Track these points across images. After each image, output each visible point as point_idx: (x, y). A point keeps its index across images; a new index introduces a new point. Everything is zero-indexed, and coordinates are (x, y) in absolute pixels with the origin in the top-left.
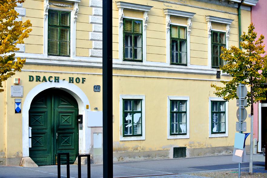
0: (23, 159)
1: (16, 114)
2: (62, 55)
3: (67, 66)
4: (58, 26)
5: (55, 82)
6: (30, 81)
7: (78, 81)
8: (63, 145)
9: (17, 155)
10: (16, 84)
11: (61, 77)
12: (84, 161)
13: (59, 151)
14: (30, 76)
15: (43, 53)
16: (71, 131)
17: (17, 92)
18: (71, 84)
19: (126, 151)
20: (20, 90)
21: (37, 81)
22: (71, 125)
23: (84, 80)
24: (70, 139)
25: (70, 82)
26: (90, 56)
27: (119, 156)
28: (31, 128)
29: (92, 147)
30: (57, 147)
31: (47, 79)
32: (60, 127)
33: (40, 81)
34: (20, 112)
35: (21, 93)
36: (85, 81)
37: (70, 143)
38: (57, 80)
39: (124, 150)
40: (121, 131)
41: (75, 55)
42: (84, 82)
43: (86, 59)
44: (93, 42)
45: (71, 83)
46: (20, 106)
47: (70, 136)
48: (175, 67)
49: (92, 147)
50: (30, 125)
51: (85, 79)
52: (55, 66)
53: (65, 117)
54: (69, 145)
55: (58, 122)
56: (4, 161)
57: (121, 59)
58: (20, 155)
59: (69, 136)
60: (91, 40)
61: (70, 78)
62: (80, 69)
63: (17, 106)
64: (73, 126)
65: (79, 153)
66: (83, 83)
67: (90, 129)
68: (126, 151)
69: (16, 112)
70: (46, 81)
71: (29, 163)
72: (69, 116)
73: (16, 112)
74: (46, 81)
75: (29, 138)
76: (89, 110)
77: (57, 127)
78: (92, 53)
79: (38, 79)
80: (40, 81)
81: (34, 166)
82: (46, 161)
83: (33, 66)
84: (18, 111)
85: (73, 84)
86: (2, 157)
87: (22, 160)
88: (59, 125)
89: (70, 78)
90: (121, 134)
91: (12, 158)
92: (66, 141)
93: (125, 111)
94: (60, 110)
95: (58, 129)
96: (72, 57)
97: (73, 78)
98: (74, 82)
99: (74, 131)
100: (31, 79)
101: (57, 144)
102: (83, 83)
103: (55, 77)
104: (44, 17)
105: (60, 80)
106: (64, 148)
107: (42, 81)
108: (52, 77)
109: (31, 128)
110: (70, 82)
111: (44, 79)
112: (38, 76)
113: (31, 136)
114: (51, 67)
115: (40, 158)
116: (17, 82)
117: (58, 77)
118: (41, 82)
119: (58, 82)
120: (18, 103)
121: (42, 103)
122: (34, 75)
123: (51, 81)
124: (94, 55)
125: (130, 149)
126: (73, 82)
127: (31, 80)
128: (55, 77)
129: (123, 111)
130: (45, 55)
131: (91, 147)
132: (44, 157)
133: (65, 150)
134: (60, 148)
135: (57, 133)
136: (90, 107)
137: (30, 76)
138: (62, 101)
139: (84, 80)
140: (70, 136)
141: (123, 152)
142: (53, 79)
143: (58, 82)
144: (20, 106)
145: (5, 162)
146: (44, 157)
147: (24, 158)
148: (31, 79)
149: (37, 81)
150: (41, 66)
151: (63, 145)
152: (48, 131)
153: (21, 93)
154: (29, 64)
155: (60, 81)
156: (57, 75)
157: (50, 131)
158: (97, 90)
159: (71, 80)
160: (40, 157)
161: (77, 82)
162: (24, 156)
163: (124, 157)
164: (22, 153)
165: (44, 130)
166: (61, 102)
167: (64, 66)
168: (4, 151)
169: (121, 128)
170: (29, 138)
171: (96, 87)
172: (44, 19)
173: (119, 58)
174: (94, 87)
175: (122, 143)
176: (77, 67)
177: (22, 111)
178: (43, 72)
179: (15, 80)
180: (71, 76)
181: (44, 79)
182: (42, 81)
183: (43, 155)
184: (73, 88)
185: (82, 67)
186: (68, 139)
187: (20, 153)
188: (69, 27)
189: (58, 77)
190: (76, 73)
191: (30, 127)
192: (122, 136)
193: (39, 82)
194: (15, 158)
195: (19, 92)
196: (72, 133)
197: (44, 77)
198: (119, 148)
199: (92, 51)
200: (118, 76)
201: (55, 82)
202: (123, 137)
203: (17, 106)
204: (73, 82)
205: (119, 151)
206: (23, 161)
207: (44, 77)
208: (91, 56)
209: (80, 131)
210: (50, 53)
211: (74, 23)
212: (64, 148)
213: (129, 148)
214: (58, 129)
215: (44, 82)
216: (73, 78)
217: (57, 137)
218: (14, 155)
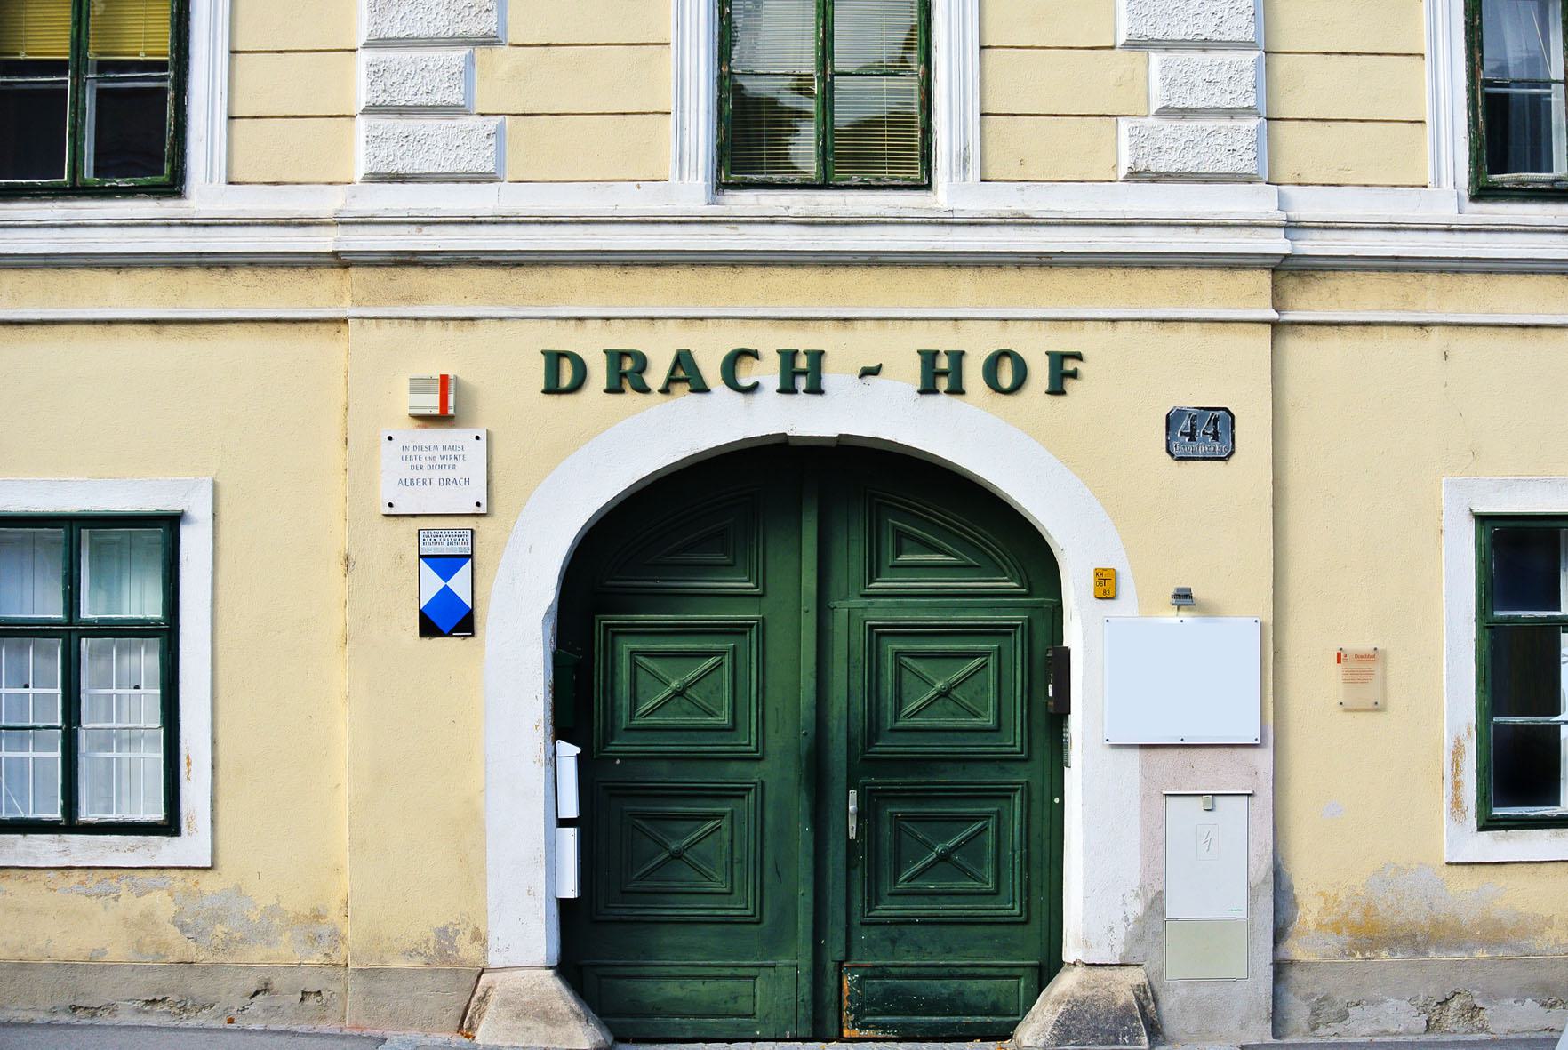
1: (426, 641)
2: (855, 179)
3: (894, 264)
5: (787, 388)
6: (552, 388)
8: (920, 884)
9: (442, 953)
10: (426, 420)
12: (1055, 1018)
13: (875, 932)
14: (554, 359)
15: (670, 172)
16: (988, 776)
17: (436, 475)
18: (942, 401)
19: (1516, 948)
20: (459, 464)
21: (614, 389)
22: (733, 729)
23: (1070, 365)
24: (990, 839)
25: (928, 389)
26: (1123, 172)
27: (1432, 989)
28: (578, 750)
29: (1156, 903)
30: (857, 905)
31: (711, 370)
32: (883, 747)
33: (645, 390)
34: (465, 624)
35: (467, 481)
36: (1074, 375)
37: (989, 872)
38: (802, 373)
39: (1485, 943)
40: (1457, 785)
41: (974, 174)
42: (1070, 384)
43: (1084, 197)
44: (1156, 58)
45: (942, 399)
46: (460, 584)
47: (987, 816)
48: (204, 80)
49: (1156, 903)
50: (563, 727)
51: (1078, 357)
52: (779, 271)
53: (669, 662)
55: (860, 706)
56: (337, 988)
57: (1447, 185)
58: (467, 951)
59: (973, 819)
60: (1133, 45)
61: (929, 358)
62: (1032, 277)
63: (432, 584)
64: (1013, 741)
66: (1057, 389)
67: (1136, 753)
68: (1516, 948)
69: (428, 627)
70: (701, 388)
71: (520, 1015)
72: (977, 661)
73: (428, 627)
74: (701, 388)
75: (564, 823)
76: (1125, 607)
77: (850, 742)
78: (1135, 147)
79: (626, 372)
80: (645, 390)
81: (550, 1040)
82: (744, 1004)
83: (578, 276)
84: (448, 620)
85: (955, 399)
86: (317, 958)
87: (479, 993)
88: (873, 730)
89: (929, 358)
90: (1457, 803)
91: (397, 971)
92: (944, 858)
93: (1499, 614)
94: (880, 612)
95: (867, 763)
97: (957, 357)
98: (603, 359)
99: (1019, 776)
100: (562, 373)
101: (857, 873)
102: (1057, 389)
103: (788, 357)
106: (922, 908)
107: (665, 391)
108: (755, 355)
109: (578, 750)
110: (928, 389)
111: (685, 372)
112: (623, 354)
113: (570, 809)
114: (751, 278)
115: (698, 984)
116: (431, 404)
117: (817, 357)
118: (656, 397)
119: (815, 389)
120: (446, 564)
121: (723, 558)
122: (593, 347)
123: (745, 381)
124: (1162, 166)
125: (1550, 934)
126: (957, 389)
127: (566, 379)
128: (788, 357)
129: (1483, 610)
130: (691, 188)
131: (1137, 908)
132: (727, 972)
133: (932, 930)
134: (889, 908)
135: (853, 794)
136: (1127, 586)
137: (554, 359)
138: (906, 544)
139: (1070, 365)
140: (987, 816)
141: (1481, 954)
142: (767, 373)
143: (815, 389)
144: (460, 584)
145: (343, 997)
146: (727, 972)
147: (499, 976)
148: (562, 373)
149: (614, 389)
150: (656, 270)
151: (920, 884)
152: (778, 774)
153: (467, 481)
154: (547, 264)
155: (828, 380)
156: (802, 341)
157: (792, 775)
159: (940, 374)
160: (690, 971)
162: (494, 959)
163: (1493, 996)
164: (478, 936)
165: (734, 767)
166: (899, 552)
167: (869, 265)
168: (334, 914)
169: (1457, 752)
171: (1185, 424)
173: (1429, 178)
174: (1172, 421)
175: (1466, 886)
176: (1000, 265)
177: (485, 621)
178: (657, 317)
179: (413, 390)
180: (943, 340)
181: (685, 372)
182: (665, 391)
183: (730, 956)
185: (1045, 261)
186: (967, 840)
187: (463, 941)
189: (817, 357)
190: (977, 318)
191: (561, 744)
192: (1472, 822)
193: (631, 397)
194: (414, 973)
195: (451, 475)
196: (1004, 794)
198: (1436, 924)
199: (377, 73)
200: (1421, 325)
201: (787, 388)
202: (1482, 828)
203: (432, 584)
204: (957, 389)
205: (1439, 947)
206: (483, 999)
208: (1135, 176)
212: (922, 908)
213: (1549, 922)
214: (864, 764)
215: (683, 398)
216: (957, 357)
217: (852, 823)
218: (410, 954)
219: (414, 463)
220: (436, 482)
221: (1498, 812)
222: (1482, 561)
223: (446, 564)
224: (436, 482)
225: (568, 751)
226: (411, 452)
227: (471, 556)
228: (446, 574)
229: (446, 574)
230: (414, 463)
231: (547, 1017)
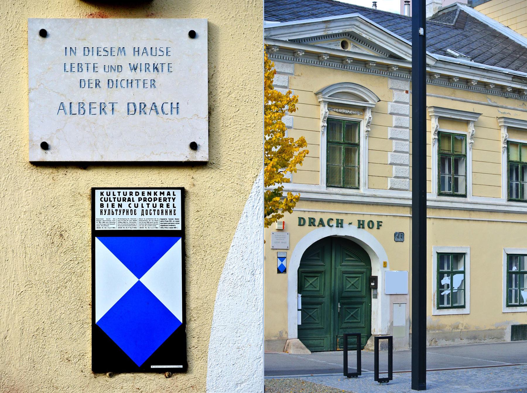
0: (288, 341)
2: (348, 187)
3: (355, 203)
4: (342, 143)
5: (337, 227)
6: (300, 225)
7: (371, 226)
8: (348, 321)
9: (280, 336)
10: (279, 230)
11: (347, 219)
13: (342, 330)
14: (300, 219)
16: (359, 300)
23: (380, 224)
25: (359, 227)
26: (389, 188)
29: (392, 323)
32: (344, 294)
33: (315, 226)
34: (285, 271)
36: (381, 225)
37: (359, 318)
38: (340, 224)
39: (439, 329)
41: (367, 187)
42: (380, 227)
43: (384, 193)
44: (394, 167)
45: (361, 229)
46: (284, 263)
47: (359, 308)
49: (392, 323)
50: (299, 292)
51: (382, 222)
54: (355, 321)
57: (434, 193)
58: (285, 336)
59: (357, 308)
60: (390, 164)
61: (359, 221)
62: (375, 207)
63: (280, 263)
64: (364, 293)
65: (372, 333)
66: (378, 228)
67: (389, 296)
69: (279, 271)
70: (324, 226)
71: (297, 348)
73: (279, 271)
74: (324, 226)
75: (298, 310)
76: (388, 269)
78: (391, 183)
79: (312, 222)
80: (315, 226)
82: (322, 345)
84: (282, 270)
85: (363, 230)
87: (287, 344)
89: (359, 221)
90: (434, 304)
92: (352, 316)
94: (344, 269)
95: (341, 298)
96: (362, 191)
97: (363, 221)
99: (365, 300)
102: (378, 228)
103: (338, 220)
104: (321, 129)
105: (345, 224)
107: (318, 226)
108: (332, 219)
110: (359, 227)
111: (321, 223)
112: (313, 218)
113: (300, 308)
114: (332, 205)
116: (281, 227)
117: (342, 220)
118: (316, 227)
119: (342, 227)
120: (282, 259)
121: (318, 258)
122: (306, 216)
123: (331, 225)
124: (395, 187)
125: (447, 328)
127: (302, 223)
128: (338, 220)
130: (323, 187)
131: (389, 324)
134: (344, 325)
136: (388, 265)
137: (300, 219)
139: (380, 224)
140: (359, 308)
141: (437, 332)
142: (334, 223)
143: (342, 227)
144: (284, 263)
147: (290, 340)
148: (301, 222)
151: (348, 321)
152: (326, 300)
156: (340, 217)
158: (399, 240)
159: (361, 225)
161: (369, 227)
162: (289, 337)
163: (439, 339)
164: (286, 333)
165: (320, 299)
169: (434, 295)
170: (298, 310)
171: (397, 235)
172: (321, 133)
174: (395, 234)
176: (370, 204)
177: (288, 270)
180: (361, 218)
181: (321, 223)
182: (318, 226)
184: (364, 236)
187: (284, 333)
188: (358, 145)
189: (342, 220)
190: (369, 214)
193: (312, 227)
194: (276, 340)
196: (361, 303)
197: (321, 220)
201: (337, 227)
203: (280, 263)
206: (288, 345)
207: (321, 220)
208: (391, 189)
209: (373, 300)
210: (330, 183)
211: (365, 139)
213: (446, 326)
214: (341, 298)
215: (321, 228)
216: (363, 221)
218: (275, 337)
221: (440, 306)
222: (438, 261)
223: (139, 248)
225: (300, 295)
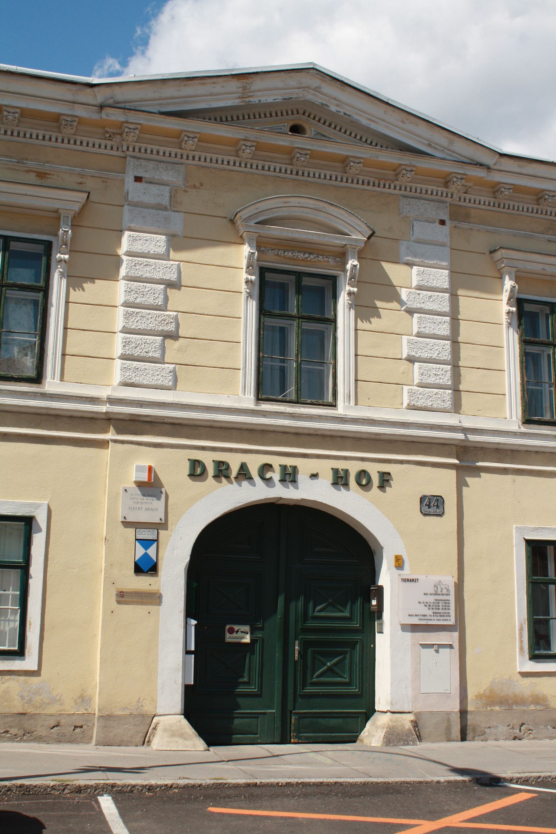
0: (155, 720)
2: (309, 401)
4: (294, 317)
7: (364, 482)
8: (323, 679)
11: (305, 467)
12: (383, 734)
21: (217, 477)
23: (386, 478)
24: (347, 661)
31: (254, 472)
32: (310, 624)
33: (227, 477)
40: (521, 642)
46: (151, 552)
50: (189, 613)
54: (339, 679)
57: (514, 418)
63: (140, 551)
65: (376, 708)
66: (382, 487)
70: (250, 478)
78: (410, 396)
79: (222, 471)
84: (147, 567)
87: (153, 726)
89: (336, 471)
90: (521, 649)
91: (118, 716)
92: (330, 669)
96: (341, 410)
97: (346, 472)
104: (243, 288)
105: (302, 477)
108: (271, 466)
113: (193, 649)
117: (295, 468)
120: (146, 543)
123: (268, 476)
124: (419, 404)
127: (199, 471)
128: (284, 468)
130: (248, 400)
135: (297, 642)
141: (532, 707)
151: (323, 679)
156: (289, 462)
158: (432, 510)
159: (340, 480)
161: (359, 484)
169: (521, 629)
170: (188, 652)
172: (244, 296)
174: (422, 499)
180: (341, 465)
184: (351, 504)
188: (334, 321)
192: (527, 656)
195: (150, 506)
197: (243, 468)
203: (140, 551)
204: (346, 485)
206: (155, 728)
207: (243, 468)
209: (377, 635)
210: (262, 393)
211: (347, 310)
217: (296, 655)
219: (135, 500)
220: (144, 509)
221: (537, 652)
222: (528, 558)
224: (144, 509)
225: (194, 622)
226: (134, 496)
227: (157, 540)
228: (146, 548)
229: (146, 548)
230: (135, 500)
231: (182, 736)
